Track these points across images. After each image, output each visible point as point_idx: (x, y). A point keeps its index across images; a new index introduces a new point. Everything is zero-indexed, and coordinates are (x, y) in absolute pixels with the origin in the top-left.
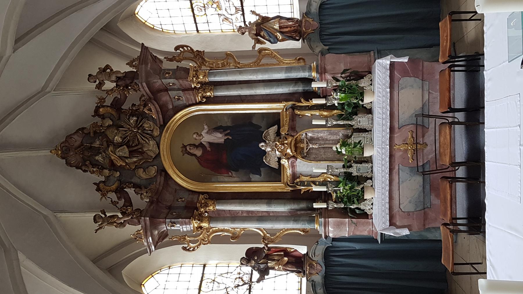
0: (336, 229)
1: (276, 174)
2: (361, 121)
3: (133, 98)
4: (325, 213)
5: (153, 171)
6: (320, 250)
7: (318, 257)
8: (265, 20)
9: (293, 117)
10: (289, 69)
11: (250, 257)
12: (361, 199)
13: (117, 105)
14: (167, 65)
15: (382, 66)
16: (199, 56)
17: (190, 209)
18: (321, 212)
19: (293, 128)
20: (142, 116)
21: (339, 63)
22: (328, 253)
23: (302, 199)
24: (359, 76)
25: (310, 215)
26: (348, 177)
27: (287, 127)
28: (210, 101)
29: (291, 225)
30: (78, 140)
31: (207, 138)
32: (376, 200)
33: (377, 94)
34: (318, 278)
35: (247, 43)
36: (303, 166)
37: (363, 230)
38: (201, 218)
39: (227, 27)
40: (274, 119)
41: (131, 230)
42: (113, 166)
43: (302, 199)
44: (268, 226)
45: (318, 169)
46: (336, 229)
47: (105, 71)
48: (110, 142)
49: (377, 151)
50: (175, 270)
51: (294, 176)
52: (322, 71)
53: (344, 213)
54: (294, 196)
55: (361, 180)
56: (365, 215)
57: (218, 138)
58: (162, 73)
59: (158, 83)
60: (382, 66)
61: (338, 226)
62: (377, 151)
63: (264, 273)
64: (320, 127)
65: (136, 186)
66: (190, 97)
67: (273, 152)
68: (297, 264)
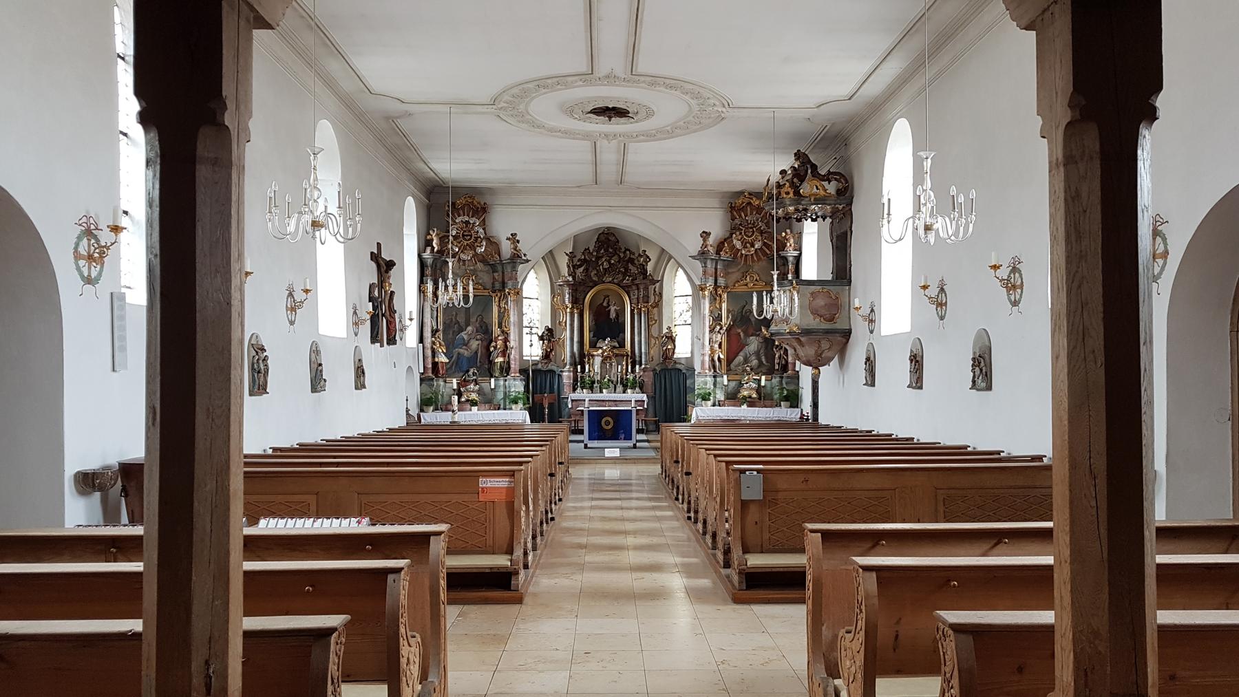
0: (567, 377)
1: (593, 345)
2: (620, 388)
3: (633, 269)
4: (575, 371)
5: (595, 279)
6: (555, 368)
7: (550, 367)
8: (674, 341)
9: (623, 356)
10: (648, 353)
11: (550, 331)
12: (582, 388)
13: (631, 261)
14: (651, 288)
15: (644, 397)
16: (658, 304)
17: (577, 301)
18: (575, 371)
19: (617, 355)
20: (625, 274)
21: (648, 379)
22: (552, 372)
23: (581, 359)
24: (641, 388)
25: (574, 364)
26: (593, 382)
27: (619, 351)
28: (632, 311)
29: (568, 354)
30: (612, 238)
31: (613, 309)
32: (583, 394)
33: (633, 396)
34: (540, 366)
35: (665, 331)
36: (598, 360)
37: (567, 389)
38: (572, 308)
39: (676, 315)
40: (622, 345)
41: (565, 270)
42: (598, 258)
43: (581, 359)
44: (568, 342)
45: (597, 368)
46: (567, 377)
47: (648, 259)
48: (611, 258)
49: (606, 395)
50: (536, 282)
51: (593, 356)
52: (644, 370)
53: (575, 380)
54: (582, 355)
55: (591, 389)
56: (574, 390)
57: (613, 315)
58: (646, 289)
59: (641, 287)
60: (644, 397)
61: (569, 377)
62: (606, 395)
63: (541, 338)
64: (617, 369)
65: (586, 270)
66: (635, 301)
67: (606, 344)
68: (546, 356)
